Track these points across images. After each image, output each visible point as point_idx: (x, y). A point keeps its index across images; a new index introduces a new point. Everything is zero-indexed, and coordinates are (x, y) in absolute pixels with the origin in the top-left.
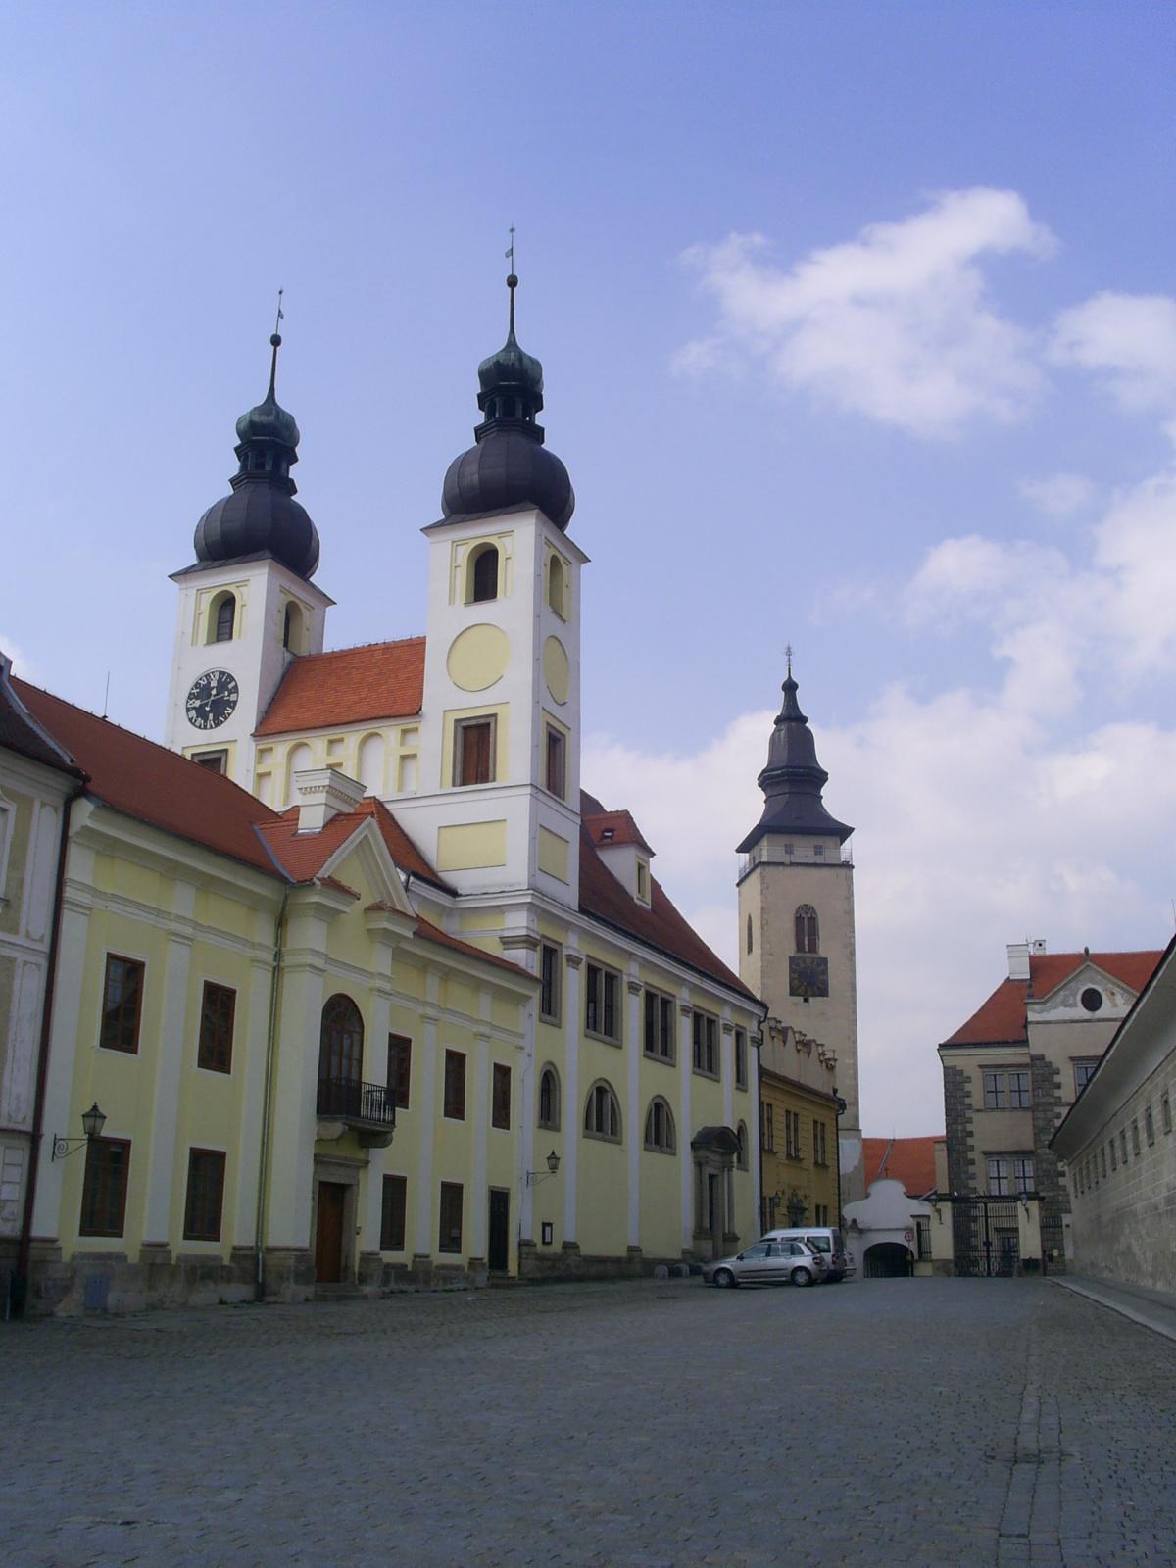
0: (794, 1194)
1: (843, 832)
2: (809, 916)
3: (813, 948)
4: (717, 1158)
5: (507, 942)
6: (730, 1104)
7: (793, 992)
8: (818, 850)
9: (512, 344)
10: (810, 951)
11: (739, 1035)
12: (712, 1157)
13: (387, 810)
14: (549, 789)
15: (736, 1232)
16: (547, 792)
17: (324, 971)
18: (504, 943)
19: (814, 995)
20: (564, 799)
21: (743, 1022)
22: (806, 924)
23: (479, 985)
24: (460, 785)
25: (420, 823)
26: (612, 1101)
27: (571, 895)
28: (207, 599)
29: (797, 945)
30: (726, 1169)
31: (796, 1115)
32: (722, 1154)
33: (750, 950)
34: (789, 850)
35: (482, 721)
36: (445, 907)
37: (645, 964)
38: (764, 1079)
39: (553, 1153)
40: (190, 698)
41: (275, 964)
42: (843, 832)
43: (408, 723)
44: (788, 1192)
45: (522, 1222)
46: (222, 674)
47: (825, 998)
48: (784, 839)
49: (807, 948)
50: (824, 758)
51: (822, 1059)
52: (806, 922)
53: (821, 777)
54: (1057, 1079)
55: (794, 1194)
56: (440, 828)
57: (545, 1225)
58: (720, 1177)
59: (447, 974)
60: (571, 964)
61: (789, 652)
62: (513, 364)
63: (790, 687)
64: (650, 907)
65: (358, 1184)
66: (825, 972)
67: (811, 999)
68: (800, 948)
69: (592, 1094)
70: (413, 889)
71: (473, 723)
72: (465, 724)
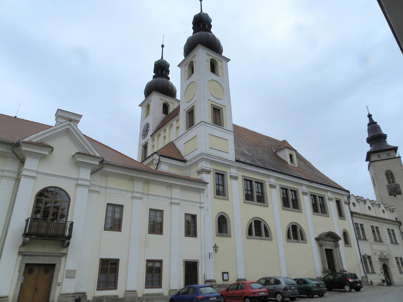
0: (382, 253)
1: (395, 149)
2: (390, 173)
3: (394, 182)
4: (332, 243)
5: (200, 172)
6: (333, 223)
7: (390, 195)
8: (388, 155)
10: (393, 183)
11: (338, 203)
12: (327, 242)
13: (174, 144)
14: (214, 123)
15: (345, 268)
16: (214, 124)
17: (35, 177)
18: (198, 173)
19: (397, 194)
20: (223, 127)
21: (339, 197)
22: (390, 175)
23: (170, 186)
24: (188, 129)
25: (179, 145)
26: (264, 225)
27: (231, 156)
28: (146, 107)
29: (388, 181)
30: (337, 247)
31: (377, 227)
32: (334, 242)
33: (375, 186)
34: (379, 156)
35: (191, 109)
36: (183, 167)
37: (277, 179)
38: (354, 215)
39: (215, 245)
40: (142, 133)
41: (17, 177)
42: (395, 149)
43: (176, 118)
44: (379, 253)
45: (207, 272)
46: (147, 124)
47: (401, 195)
48: (377, 154)
49: (391, 182)
50: (384, 131)
51: (387, 209)
52: (389, 175)
53: (385, 137)
55: (382, 253)
56: (184, 144)
57: (223, 273)
58: (334, 250)
59: (147, 182)
60: (232, 178)
61: (367, 107)
62: (198, 16)
63: (370, 116)
64: (297, 166)
65: (60, 264)
66: (399, 187)
67: (397, 196)
68: (389, 182)
69: (251, 223)
70: (161, 160)
71: (190, 111)
72: (188, 112)
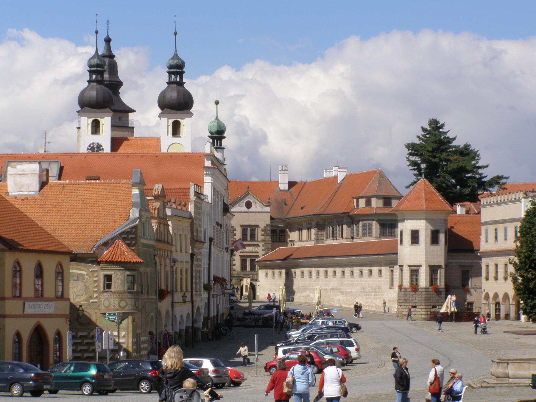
9: (176, 56)
53: (120, 84)
54: (235, 232)
61: (108, 23)
